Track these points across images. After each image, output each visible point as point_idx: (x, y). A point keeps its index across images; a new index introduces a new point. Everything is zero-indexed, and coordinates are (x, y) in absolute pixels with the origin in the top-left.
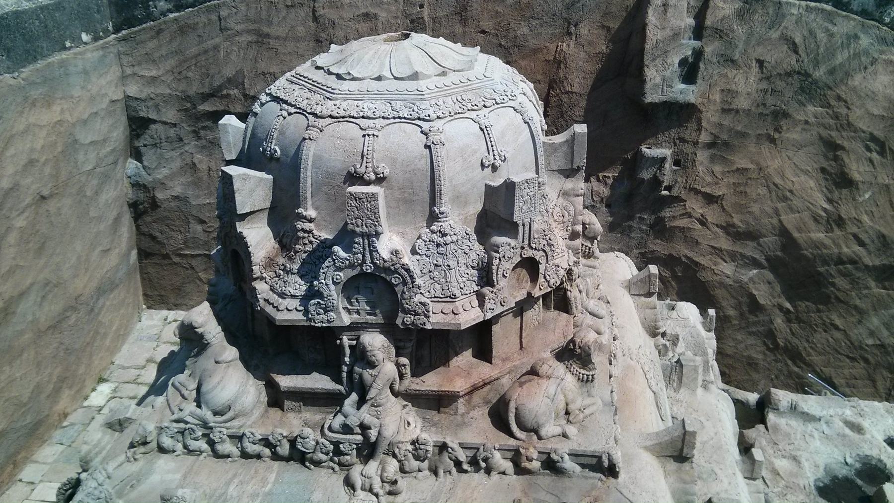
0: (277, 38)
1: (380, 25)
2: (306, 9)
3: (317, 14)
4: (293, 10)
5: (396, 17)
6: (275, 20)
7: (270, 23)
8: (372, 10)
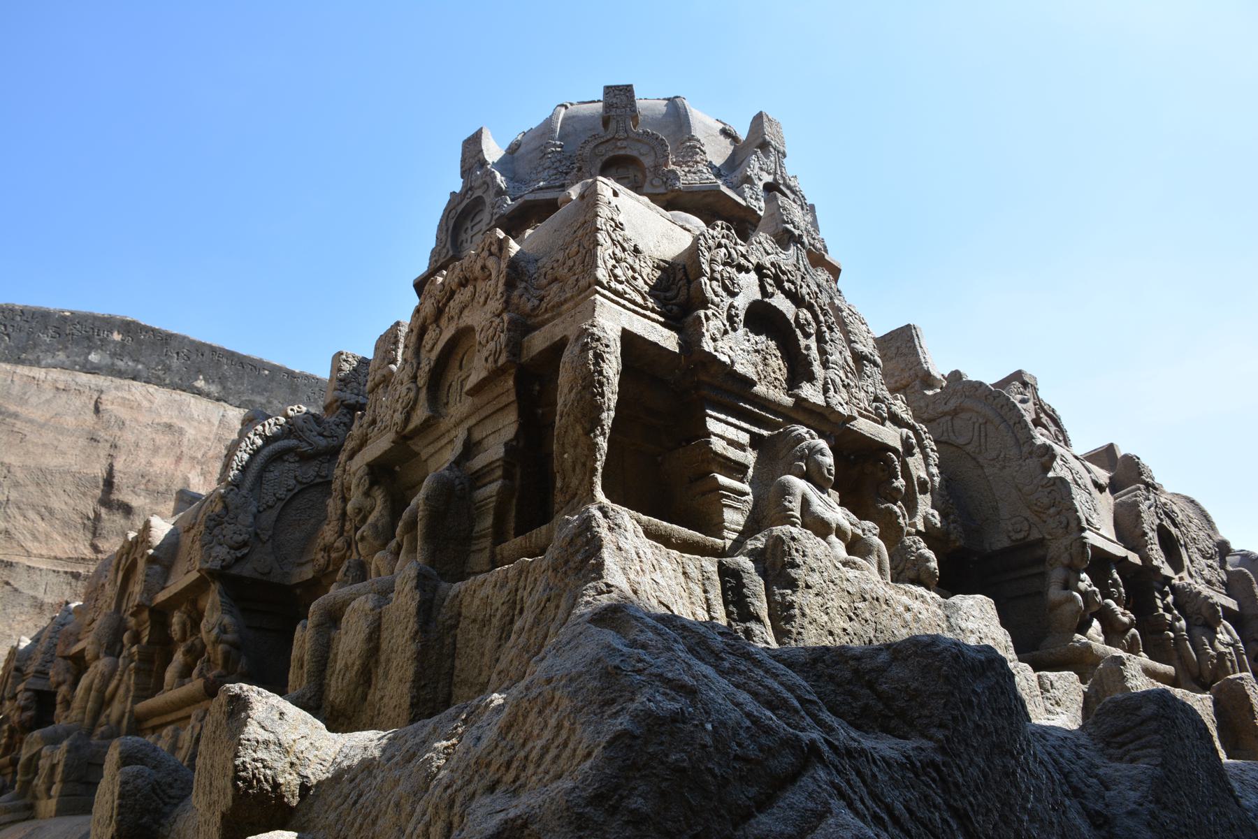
0: (31, 421)
1: (185, 441)
2: (84, 398)
3: (102, 407)
4: (64, 396)
5: (207, 439)
6: (34, 400)
7: (22, 401)
8: (177, 422)
